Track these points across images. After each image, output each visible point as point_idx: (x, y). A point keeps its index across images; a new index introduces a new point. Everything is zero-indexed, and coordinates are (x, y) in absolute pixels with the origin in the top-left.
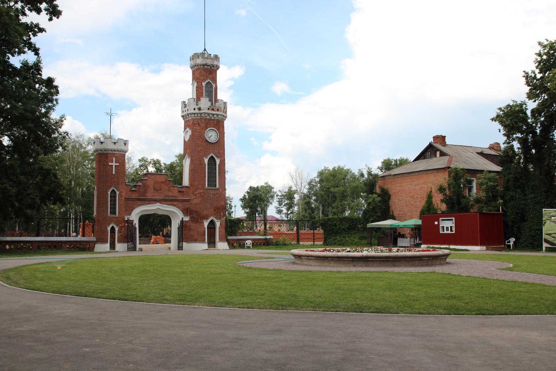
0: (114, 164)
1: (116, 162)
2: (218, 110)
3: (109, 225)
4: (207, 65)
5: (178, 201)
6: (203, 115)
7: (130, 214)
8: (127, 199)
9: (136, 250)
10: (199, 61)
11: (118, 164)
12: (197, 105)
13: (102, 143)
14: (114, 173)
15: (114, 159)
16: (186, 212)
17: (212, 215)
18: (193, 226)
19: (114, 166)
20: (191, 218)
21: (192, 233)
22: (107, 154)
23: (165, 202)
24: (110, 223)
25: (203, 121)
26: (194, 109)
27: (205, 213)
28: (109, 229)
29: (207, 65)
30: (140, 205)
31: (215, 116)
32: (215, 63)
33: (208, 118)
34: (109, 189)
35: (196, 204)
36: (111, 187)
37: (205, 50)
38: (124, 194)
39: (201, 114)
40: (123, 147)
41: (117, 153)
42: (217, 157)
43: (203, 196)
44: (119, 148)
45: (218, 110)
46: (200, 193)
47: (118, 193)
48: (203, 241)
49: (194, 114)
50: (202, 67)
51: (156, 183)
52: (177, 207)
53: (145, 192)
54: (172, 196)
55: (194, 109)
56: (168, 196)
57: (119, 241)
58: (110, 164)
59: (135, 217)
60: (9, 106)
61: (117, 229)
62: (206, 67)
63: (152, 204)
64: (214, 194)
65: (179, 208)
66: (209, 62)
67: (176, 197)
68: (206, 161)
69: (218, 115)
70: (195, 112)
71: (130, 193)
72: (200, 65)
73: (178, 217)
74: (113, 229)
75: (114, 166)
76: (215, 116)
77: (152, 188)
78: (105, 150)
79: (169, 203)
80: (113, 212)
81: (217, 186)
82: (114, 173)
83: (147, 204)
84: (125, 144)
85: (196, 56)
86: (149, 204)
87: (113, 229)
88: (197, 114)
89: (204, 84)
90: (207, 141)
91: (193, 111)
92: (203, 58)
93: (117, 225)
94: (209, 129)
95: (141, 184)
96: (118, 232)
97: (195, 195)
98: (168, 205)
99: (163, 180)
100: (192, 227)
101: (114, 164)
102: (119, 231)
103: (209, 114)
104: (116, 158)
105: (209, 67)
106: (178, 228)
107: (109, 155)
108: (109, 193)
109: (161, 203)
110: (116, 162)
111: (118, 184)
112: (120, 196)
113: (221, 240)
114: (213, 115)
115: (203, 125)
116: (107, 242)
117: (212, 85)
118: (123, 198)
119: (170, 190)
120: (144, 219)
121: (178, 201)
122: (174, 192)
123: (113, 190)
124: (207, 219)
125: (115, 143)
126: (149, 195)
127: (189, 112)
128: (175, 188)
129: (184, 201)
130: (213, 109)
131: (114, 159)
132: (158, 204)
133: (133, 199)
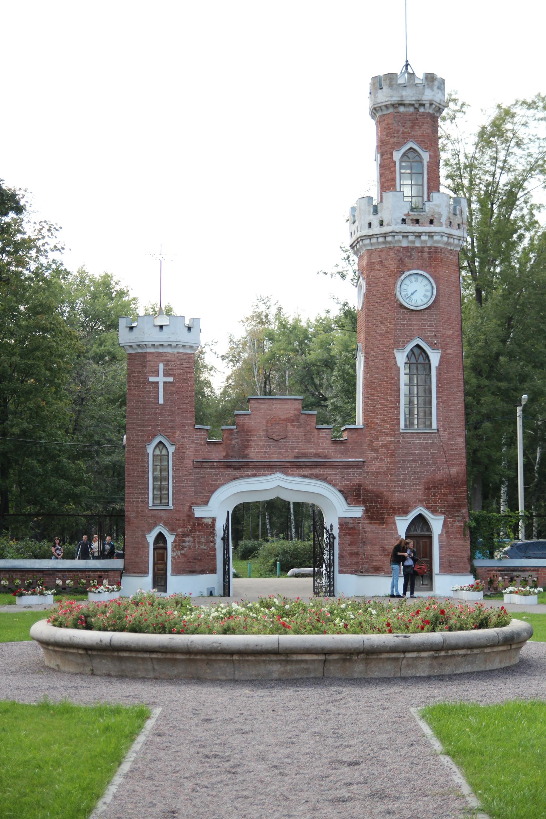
0: (161, 379)
1: (166, 374)
2: (431, 222)
3: (150, 531)
4: (404, 105)
5: (332, 466)
6: (389, 239)
7: (206, 503)
8: (199, 465)
9: (229, 596)
10: (385, 96)
11: (171, 379)
14: (161, 401)
15: (161, 366)
16: (353, 495)
17: (420, 502)
18: (372, 530)
20: (367, 511)
21: (368, 549)
22: (143, 356)
23: (297, 471)
24: (155, 526)
25: (392, 253)
26: (370, 224)
27: (397, 496)
28: (151, 538)
29: (404, 105)
32: (428, 95)
33: (405, 244)
34: (150, 441)
35: (378, 473)
36: (154, 435)
37: (407, 65)
38: (189, 453)
39: (385, 235)
40: (185, 338)
41: (169, 350)
42: (433, 346)
43: (393, 452)
44: (173, 339)
45: (431, 222)
46: (387, 445)
47: (171, 450)
49: (370, 237)
50: (391, 110)
51: (272, 422)
52: (330, 483)
53: (245, 445)
54: (317, 455)
55: (370, 224)
56: (305, 456)
57: (178, 571)
58: (151, 379)
59: (218, 508)
61: (170, 539)
62: (402, 109)
63: (263, 475)
64: (424, 447)
65: (334, 486)
66: (409, 95)
67: (325, 457)
68: (401, 358)
69: (431, 235)
70: (370, 232)
71: (207, 449)
72: (386, 106)
73: (337, 509)
76: (424, 238)
77: (262, 435)
79: (308, 472)
80: (161, 498)
81: (434, 426)
82: (161, 401)
83: (249, 476)
85: (378, 83)
86: (254, 476)
89: (397, 156)
90: (402, 306)
92: (391, 86)
94: (407, 273)
96: (174, 548)
97: (375, 450)
99: (292, 413)
100: (369, 536)
101: (161, 379)
105: (411, 109)
107: (149, 358)
109: (286, 473)
110: (166, 374)
111: (173, 429)
112: (179, 456)
113: (449, 568)
114: (419, 235)
115: (392, 266)
117: (419, 155)
118: (188, 463)
119: (308, 440)
120: (240, 515)
121: (332, 466)
122: (322, 444)
124: (406, 513)
125: (161, 327)
126: (255, 453)
128: (322, 434)
129: (348, 466)
130: (417, 221)
131: (161, 366)
132: (279, 475)
133: (211, 465)
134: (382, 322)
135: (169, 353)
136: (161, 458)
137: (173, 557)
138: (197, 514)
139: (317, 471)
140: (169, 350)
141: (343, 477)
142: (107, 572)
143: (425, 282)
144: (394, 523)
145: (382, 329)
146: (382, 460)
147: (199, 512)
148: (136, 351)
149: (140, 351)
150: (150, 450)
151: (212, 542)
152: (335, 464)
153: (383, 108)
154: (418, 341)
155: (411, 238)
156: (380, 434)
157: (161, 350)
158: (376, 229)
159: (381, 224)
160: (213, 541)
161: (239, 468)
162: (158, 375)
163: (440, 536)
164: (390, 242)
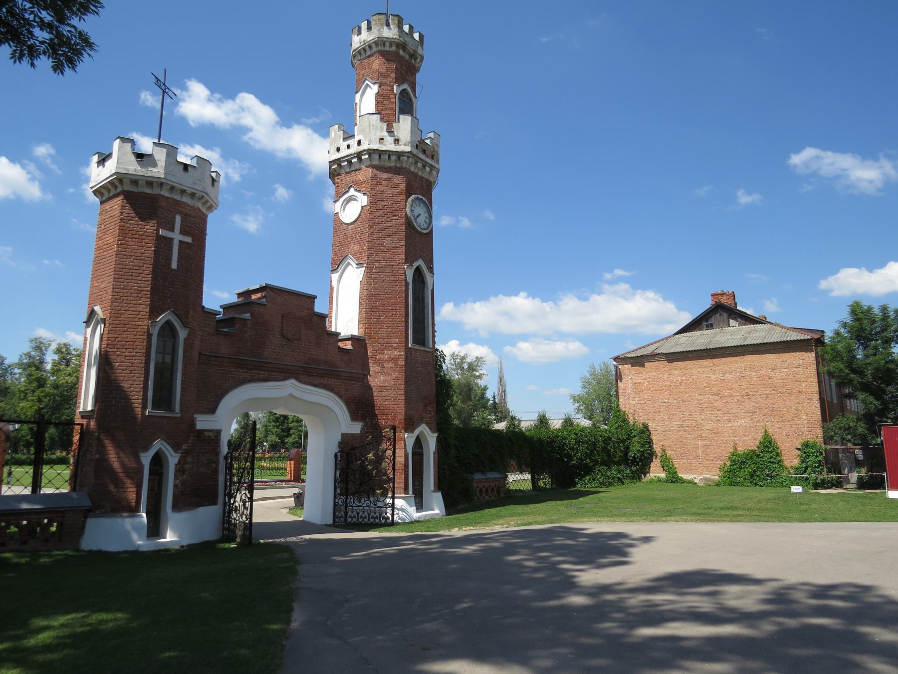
3: (146, 449)
7: (212, 410)
11: (189, 240)
12: (390, 131)
14: (174, 266)
15: (178, 219)
22: (155, 198)
28: (146, 459)
31: (428, 169)
45: (432, 157)
47: (182, 334)
49: (380, 153)
61: (173, 459)
62: (401, 52)
65: (341, 397)
74: (158, 461)
82: (174, 266)
84: (213, 185)
87: (158, 461)
88: (390, 153)
91: (376, 146)
93: (176, 447)
95: (247, 316)
97: (380, 363)
102: (180, 470)
104: (185, 217)
106: (336, 456)
110: (183, 232)
123: (168, 323)
127: (365, 146)
131: (178, 219)
134: (389, 236)
135: (189, 205)
137: (175, 486)
138: (199, 426)
139: (325, 381)
140: (186, 199)
141: (347, 390)
142: (63, 512)
143: (425, 209)
145: (388, 242)
146: (388, 374)
147: (203, 422)
148: (140, 190)
149: (148, 191)
151: (214, 462)
152: (343, 374)
153: (387, 44)
155: (420, 165)
156: (389, 346)
157: (178, 197)
158: (389, 145)
159: (397, 141)
160: (217, 462)
161: (251, 369)
162: (172, 230)
163: (434, 453)
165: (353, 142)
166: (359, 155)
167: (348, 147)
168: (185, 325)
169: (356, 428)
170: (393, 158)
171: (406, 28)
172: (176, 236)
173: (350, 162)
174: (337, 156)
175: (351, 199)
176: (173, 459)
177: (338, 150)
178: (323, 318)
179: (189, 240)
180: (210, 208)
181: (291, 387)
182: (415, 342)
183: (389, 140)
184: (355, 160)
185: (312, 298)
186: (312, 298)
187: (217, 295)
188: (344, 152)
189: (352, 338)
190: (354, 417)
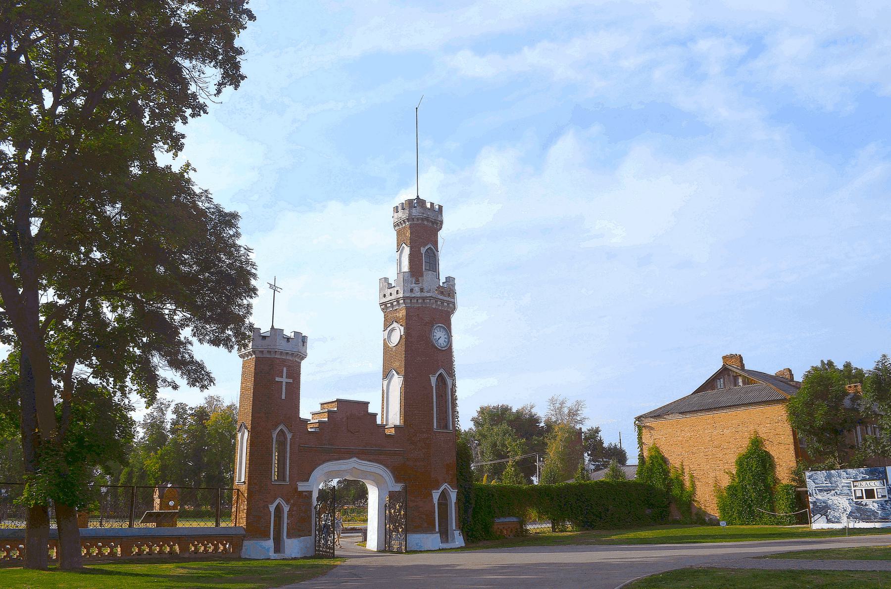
0: (284, 380)
3: (272, 503)
11: (291, 381)
13: (264, 337)
14: (283, 397)
15: (285, 369)
19: (284, 384)
26: (412, 290)
28: (272, 508)
30: (324, 462)
36: (276, 426)
39: (424, 299)
47: (289, 436)
48: (430, 529)
49: (411, 298)
52: (385, 465)
58: (277, 379)
60: (48, 296)
61: (286, 509)
62: (426, 223)
65: (387, 467)
74: (279, 509)
75: (284, 384)
78: (269, 352)
82: (283, 397)
83: (336, 460)
87: (279, 509)
88: (417, 298)
93: (287, 502)
98: (370, 461)
103: (437, 300)
104: (289, 367)
108: (274, 436)
114: (443, 302)
116: (266, 536)
131: (285, 369)
136: (282, 444)
138: (300, 489)
144: (431, 495)
147: (302, 487)
150: (274, 436)
154: (441, 371)
159: (422, 290)
160: (311, 511)
164: (426, 303)
165: (393, 291)
166: (398, 300)
167: (391, 294)
168: (290, 431)
169: (398, 487)
170: (420, 301)
171: (428, 206)
172: (284, 380)
173: (392, 304)
174: (384, 300)
175: (393, 330)
176: (286, 509)
177: (385, 296)
178: (374, 415)
179: (291, 381)
180: (303, 358)
181: (353, 463)
182: (439, 426)
183: (417, 289)
184: (395, 303)
185: (366, 404)
186: (366, 404)
187: (309, 407)
188: (388, 298)
189: (396, 427)
190: (398, 479)
